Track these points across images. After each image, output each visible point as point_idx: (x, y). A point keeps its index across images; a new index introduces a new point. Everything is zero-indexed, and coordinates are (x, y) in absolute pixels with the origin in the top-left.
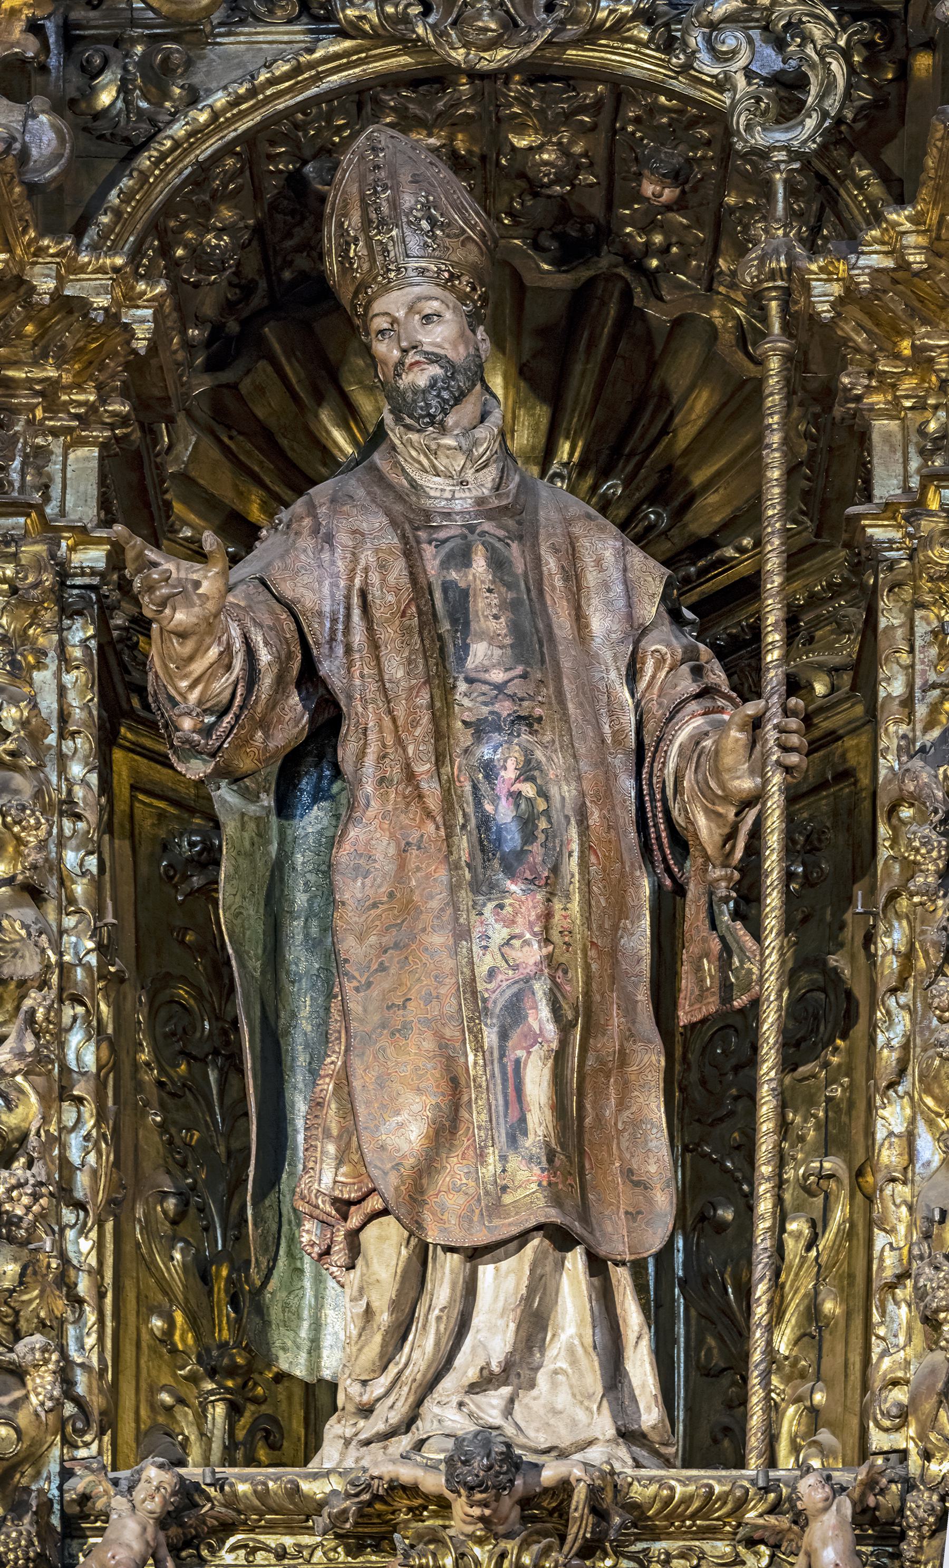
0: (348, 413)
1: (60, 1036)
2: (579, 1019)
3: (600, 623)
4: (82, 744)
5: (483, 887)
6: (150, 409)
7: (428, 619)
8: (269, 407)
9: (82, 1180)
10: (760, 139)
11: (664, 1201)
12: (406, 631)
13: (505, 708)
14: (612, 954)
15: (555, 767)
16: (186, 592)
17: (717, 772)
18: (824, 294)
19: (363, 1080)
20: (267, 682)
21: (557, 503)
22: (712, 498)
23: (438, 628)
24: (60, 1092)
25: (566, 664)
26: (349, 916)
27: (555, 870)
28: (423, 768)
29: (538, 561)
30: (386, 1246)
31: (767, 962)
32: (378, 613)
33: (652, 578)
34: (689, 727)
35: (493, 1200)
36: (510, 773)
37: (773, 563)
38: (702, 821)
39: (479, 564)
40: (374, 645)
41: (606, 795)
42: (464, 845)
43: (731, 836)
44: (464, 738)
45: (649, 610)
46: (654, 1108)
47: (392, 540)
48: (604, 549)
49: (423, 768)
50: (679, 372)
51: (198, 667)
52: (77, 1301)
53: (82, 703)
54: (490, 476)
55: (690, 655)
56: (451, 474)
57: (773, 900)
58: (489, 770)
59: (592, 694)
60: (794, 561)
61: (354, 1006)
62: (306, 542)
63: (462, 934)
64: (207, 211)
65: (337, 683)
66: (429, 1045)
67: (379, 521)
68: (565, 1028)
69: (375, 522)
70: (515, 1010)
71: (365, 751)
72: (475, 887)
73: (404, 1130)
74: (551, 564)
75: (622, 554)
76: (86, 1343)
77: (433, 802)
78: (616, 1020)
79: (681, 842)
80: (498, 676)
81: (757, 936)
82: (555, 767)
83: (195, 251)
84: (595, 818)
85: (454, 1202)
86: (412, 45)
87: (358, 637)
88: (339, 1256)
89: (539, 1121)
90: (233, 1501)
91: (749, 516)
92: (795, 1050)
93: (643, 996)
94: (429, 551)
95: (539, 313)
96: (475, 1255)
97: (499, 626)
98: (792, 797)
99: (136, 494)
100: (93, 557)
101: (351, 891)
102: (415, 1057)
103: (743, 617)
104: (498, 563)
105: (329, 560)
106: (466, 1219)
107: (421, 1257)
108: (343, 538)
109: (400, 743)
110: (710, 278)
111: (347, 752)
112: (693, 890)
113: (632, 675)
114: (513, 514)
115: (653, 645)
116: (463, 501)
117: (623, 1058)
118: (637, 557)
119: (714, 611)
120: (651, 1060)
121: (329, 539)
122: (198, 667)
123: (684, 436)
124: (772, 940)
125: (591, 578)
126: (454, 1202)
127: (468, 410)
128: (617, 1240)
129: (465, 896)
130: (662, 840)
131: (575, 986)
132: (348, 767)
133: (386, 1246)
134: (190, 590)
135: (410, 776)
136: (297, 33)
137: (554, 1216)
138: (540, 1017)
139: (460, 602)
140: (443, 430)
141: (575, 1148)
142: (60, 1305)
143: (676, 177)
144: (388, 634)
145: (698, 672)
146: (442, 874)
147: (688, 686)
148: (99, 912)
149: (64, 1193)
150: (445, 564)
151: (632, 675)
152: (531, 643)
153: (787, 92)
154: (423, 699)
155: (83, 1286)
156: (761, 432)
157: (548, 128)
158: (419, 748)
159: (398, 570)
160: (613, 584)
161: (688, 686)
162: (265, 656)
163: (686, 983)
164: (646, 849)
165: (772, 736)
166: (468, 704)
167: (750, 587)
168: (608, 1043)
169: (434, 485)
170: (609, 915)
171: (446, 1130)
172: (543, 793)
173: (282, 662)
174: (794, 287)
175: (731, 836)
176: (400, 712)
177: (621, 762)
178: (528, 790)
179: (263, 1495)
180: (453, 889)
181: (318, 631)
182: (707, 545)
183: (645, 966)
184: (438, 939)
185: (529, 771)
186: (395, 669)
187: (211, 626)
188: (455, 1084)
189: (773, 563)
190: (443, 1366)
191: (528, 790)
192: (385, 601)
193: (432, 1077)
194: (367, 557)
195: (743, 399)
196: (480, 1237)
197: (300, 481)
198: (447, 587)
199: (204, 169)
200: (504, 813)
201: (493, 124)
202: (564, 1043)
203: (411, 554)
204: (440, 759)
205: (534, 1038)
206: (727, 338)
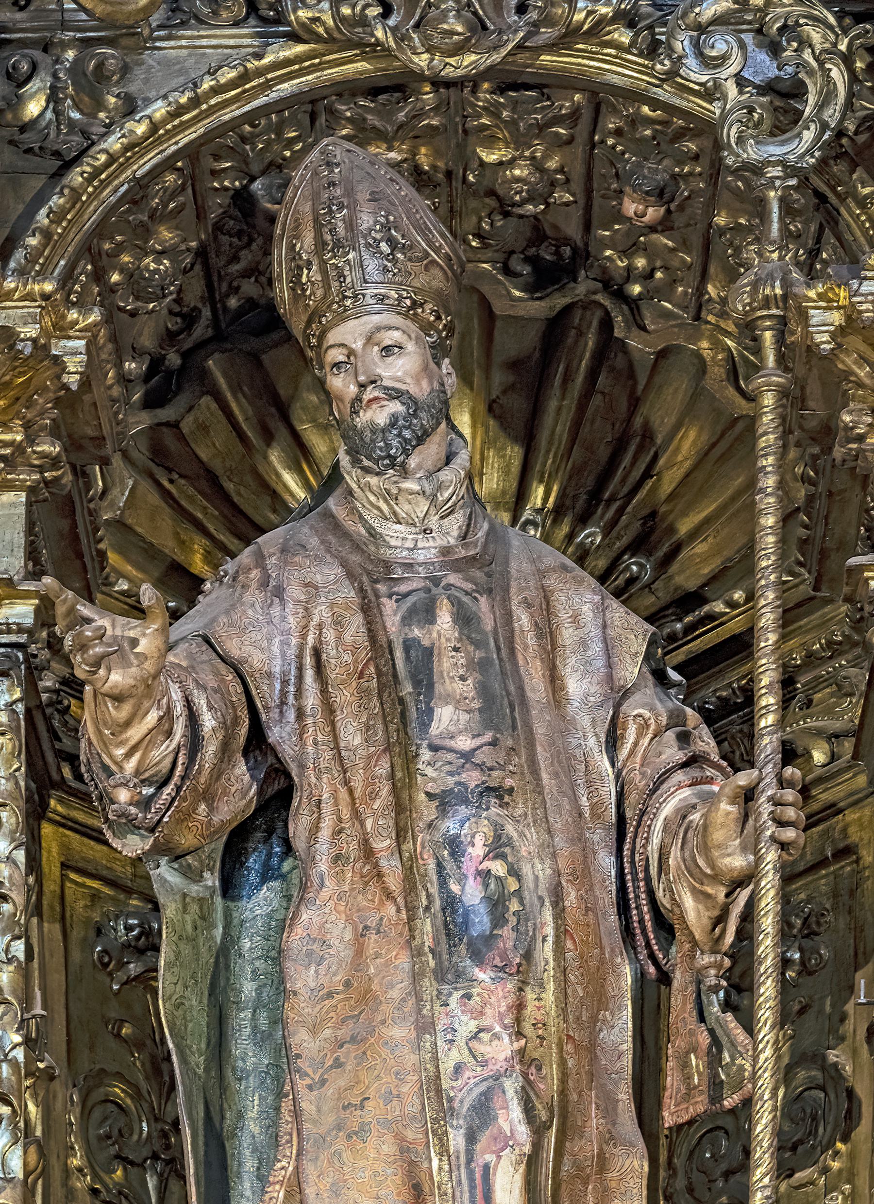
0: (301, 453)
2: (554, 1120)
3: (576, 686)
5: (448, 975)
6: (83, 450)
7: (388, 680)
8: (213, 448)
10: (753, 152)
12: (363, 693)
13: (473, 778)
14: (590, 1048)
15: (527, 841)
17: (705, 848)
18: (823, 323)
20: (210, 749)
21: (529, 553)
22: (700, 548)
23: (398, 691)
25: (540, 730)
26: (301, 1008)
27: (528, 956)
28: (382, 844)
29: (508, 617)
31: (761, 1057)
32: (333, 673)
33: (633, 635)
34: (676, 798)
36: (478, 850)
37: (768, 618)
38: (689, 902)
39: (445, 619)
40: (329, 709)
41: (583, 873)
42: (427, 928)
43: (721, 919)
44: (427, 811)
45: (631, 670)
47: (348, 593)
48: (582, 604)
49: (382, 844)
50: (662, 410)
51: (135, 733)
54: (455, 524)
55: (676, 720)
56: (411, 522)
57: (767, 989)
58: (455, 846)
59: (567, 763)
60: (789, 616)
61: (307, 1106)
62: (254, 596)
63: (425, 1026)
64: (145, 231)
65: (288, 751)
66: (389, 1148)
67: (334, 571)
68: (538, 1130)
69: (329, 573)
70: (484, 1110)
71: (318, 824)
72: (440, 975)
74: (523, 620)
75: (601, 609)
77: (394, 882)
78: (595, 1121)
79: (666, 926)
80: (465, 743)
81: (750, 1029)
82: (527, 841)
83: (131, 275)
84: (571, 898)
86: (371, 49)
87: (312, 700)
91: (740, 567)
92: (791, 1153)
93: (624, 1095)
94: (389, 605)
95: (511, 344)
97: (467, 688)
98: (788, 877)
99: (65, 542)
101: (304, 979)
103: (734, 677)
104: (464, 619)
105: (278, 617)
108: (295, 592)
109: (356, 815)
110: (698, 306)
111: (298, 827)
112: (679, 978)
113: (612, 741)
114: (481, 564)
115: (634, 708)
116: (427, 551)
117: (602, 1163)
118: (617, 612)
120: (632, 1166)
121: (279, 592)
122: (135, 733)
123: (669, 481)
124: (766, 1033)
125: (567, 635)
127: (433, 449)
129: (429, 985)
131: (549, 1084)
132: (299, 844)
134: (128, 650)
135: (368, 853)
136: (244, 37)
138: (511, 1118)
139: (423, 661)
140: (405, 472)
143: (661, 195)
145: (684, 738)
146: (404, 961)
147: (673, 753)
148: (26, 1001)
150: (407, 621)
151: (612, 741)
152: (501, 707)
153: (783, 101)
154: (383, 768)
157: (519, 141)
158: (378, 823)
159: (355, 627)
160: (593, 643)
161: (673, 753)
162: (208, 722)
163: (672, 1080)
164: (628, 933)
165: (765, 808)
166: (432, 773)
167: (741, 646)
168: (586, 1147)
172: (514, 872)
173: (228, 727)
174: (790, 315)
175: (721, 919)
176: (358, 783)
177: (600, 838)
178: (498, 868)
180: (416, 977)
181: (267, 694)
182: (692, 600)
183: (627, 1061)
184: (400, 1032)
185: (498, 847)
186: (352, 735)
187: (147, 689)
189: (768, 618)
191: (498, 868)
192: (339, 661)
194: (321, 612)
195: (733, 439)
197: (248, 529)
198: (409, 645)
199: (141, 187)
200: (472, 894)
201: (461, 136)
202: (537, 1146)
203: (369, 609)
204: (401, 834)
205: (505, 1141)
206: (717, 372)
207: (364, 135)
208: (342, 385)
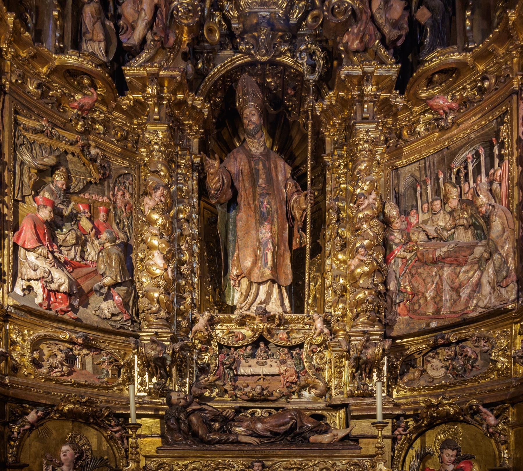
1: (192, 245)
2: (276, 246)
3: (280, 178)
4: (196, 195)
5: (261, 223)
7: (252, 175)
9: (195, 269)
11: (290, 277)
12: (248, 177)
13: (265, 191)
14: (282, 236)
17: (299, 204)
19: (241, 255)
20: (226, 185)
22: (299, 158)
24: (192, 255)
25: (275, 184)
26: (239, 228)
27: (273, 221)
28: (251, 202)
29: (270, 165)
30: (245, 283)
32: (244, 174)
33: (289, 170)
36: (265, 203)
40: (243, 180)
43: (302, 216)
44: (258, 197)
45: (289, 176)
46: (289, 262)
47: (246, 160)
48: (281, 164)
49: (251, 202)
51: (214, 181)
52: (194, 288)
53: (196, 187)
54: (262, 148)
55: (295, 184)
58: (262, 203)
61: (240, 243)
62: (232, 160)
63: (257, 231)
65: (237, 187)
66: (252, 249)
67: (244, 156)
68: (274, 248)
70: (266, 243)
71: (242, 199)
72: (260, 223)
73: (248, 263)
74: (272, 165)
75: (284, 165)
76: (196, 295)
77: (253, 209)
78: (283, 247)
79: (293, 218)
80: (264, 186)
81: (306, 234)
82: (273, 203)
84: (279, 212)
85: (256, 275)
87: (241, 179)
88: (237, 285)
89: (270, 263)
91: (305, 162)
93: (287, 244)
94: (252, 162)
96: (259, 284)
97: (263, 176)
100: (197, 160)
101: (239, 224)
102: (250, 251)
104: (264, 165)
106: (258, 278)
107: (250, 284)
108: (238, 159)
109: (247, 198)
111: (239, 199)
112: (295, 227)
113: (286, 188)
117: (284, 254)
118: (287, 165)
119: (299, 178)
120: (288, 255)
121: (236, 159)
122: (214, 181)
123: (294, 145)
125: (279, 169)
126: (256, 275)
128: (283, 282)
129: (258, 225)
130: (290, 218)
132: (239, 202)
133: (245, 283)
135: (249, 204)
137: (272, 278)
138: (270, 246)
140: (255, 139)
141: (276, 267)
142: (191, 289)
144: (246, 178)
145: (296, 187)
146: (254, 221)
147: (295, 190)
148: (198, 225)
149: (192, 271)
150: (255, 165)
151: (286, 188)
154: (251, 190)
155: (195, 286)
156: (307, 146)
158: (250, 199)
161: (295, 190)
162: (225, 181)
163: (294, 242)
164: (288, 219)
167: (305, 174)
168: (281, 251)
169: (253, 150)
170: (281, 229)
171: (255, 263)
172: (271, 207)
173: (228, 182)
175: (302, 216)
176: (247, 192)
177: (283, 203)
178: (268, 206)
180: (256, 224)
181: (234, 177)
182: (298, 167)
183: (287, 239)
184: (253, 232)
188: (256, 256)
191: (268, 206)
192: (245, 171)
193: (252, 255)
194: (242, 163)
195: (305, 137)
198: (255, 169)
200: (264, 210)
202: (274, 250)
203: (250, 163)
204: (254, 200)
205: (268, 249)
206: (302, 125)
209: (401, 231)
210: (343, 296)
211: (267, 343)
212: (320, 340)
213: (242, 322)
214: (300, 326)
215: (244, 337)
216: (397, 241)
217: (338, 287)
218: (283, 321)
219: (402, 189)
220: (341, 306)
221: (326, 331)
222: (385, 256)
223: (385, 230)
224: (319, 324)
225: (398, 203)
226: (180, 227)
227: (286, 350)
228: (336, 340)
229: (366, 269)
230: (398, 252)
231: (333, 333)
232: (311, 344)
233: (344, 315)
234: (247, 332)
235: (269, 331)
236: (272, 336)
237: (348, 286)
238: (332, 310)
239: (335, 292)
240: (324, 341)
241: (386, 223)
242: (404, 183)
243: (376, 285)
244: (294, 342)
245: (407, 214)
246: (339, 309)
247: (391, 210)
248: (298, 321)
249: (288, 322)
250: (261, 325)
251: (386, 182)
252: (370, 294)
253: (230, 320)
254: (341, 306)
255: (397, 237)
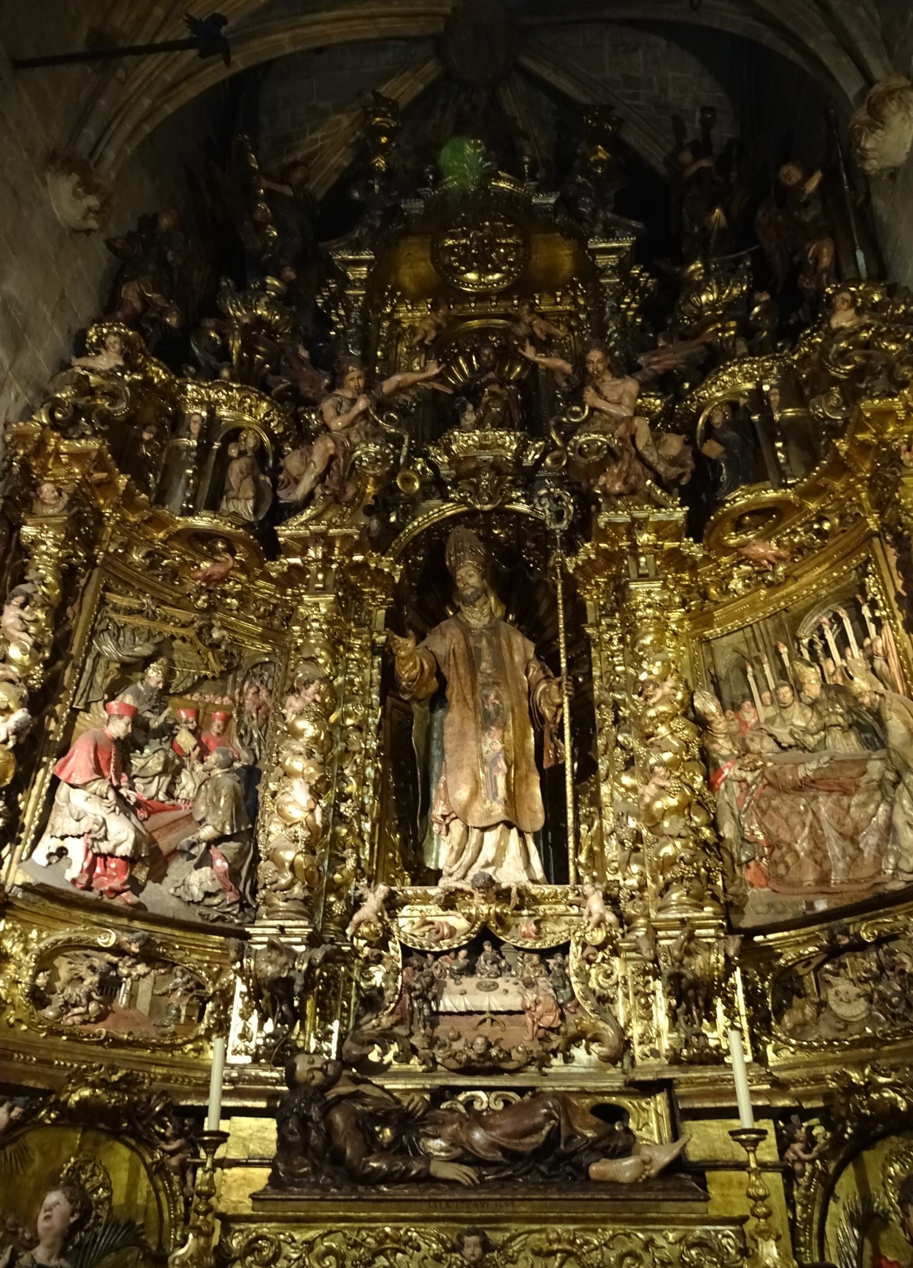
16: (405, 648)
35: (489, 813)
56: (475, 619)
86: (467, 504)
90: (406, 896)
127: (481, 601)
136: (439, 502)
157: (502, 528)
179: (416, 894)
187: (410, 657)
190: (474, 861)
196: (485, 824)
197: (437, 622)
201: (489, 527)
207: (468, 526)
208: (460, 585)
209: (730, 736)
210: (637, 850)
211: (497, 944)
212: (599, 936)
213: (449, 902)
214: (561, 908)
215: (453, 932)
216: (725, 752)
217: (625, 834)
218: (525, 899)
219: (722, 671)
220: (635, 868)
221: (610, 917)
222: (707, 778)
223: (700, 735)
224: (596, 904)
225: (718, 694)
226: (346, 739)
227: (535, 958)
228: (631, 936)
229: (673, 802)
230: (729, 770)
231: (625, 921)
232: (584, 946)
233: (642, 887)
234: (458, 921)
235: (500, 919)
236: (506, 928)
237: (644, 832)
238: (619, 877)
239: (622, 843)
240: (609, 939)
241: (701, 723)
242: (724, 662)
243: (696, 831)
244: (549, 942)
245: (736, 708)
246: (632, 875)
247: (706, 704)
248: (555, 899)
249: (537, 900)
250: (484, 909)
251: (693, 660)
252: (686, 846)
253: (426, 899)
254: (635, 868)
255: (723, 746)
